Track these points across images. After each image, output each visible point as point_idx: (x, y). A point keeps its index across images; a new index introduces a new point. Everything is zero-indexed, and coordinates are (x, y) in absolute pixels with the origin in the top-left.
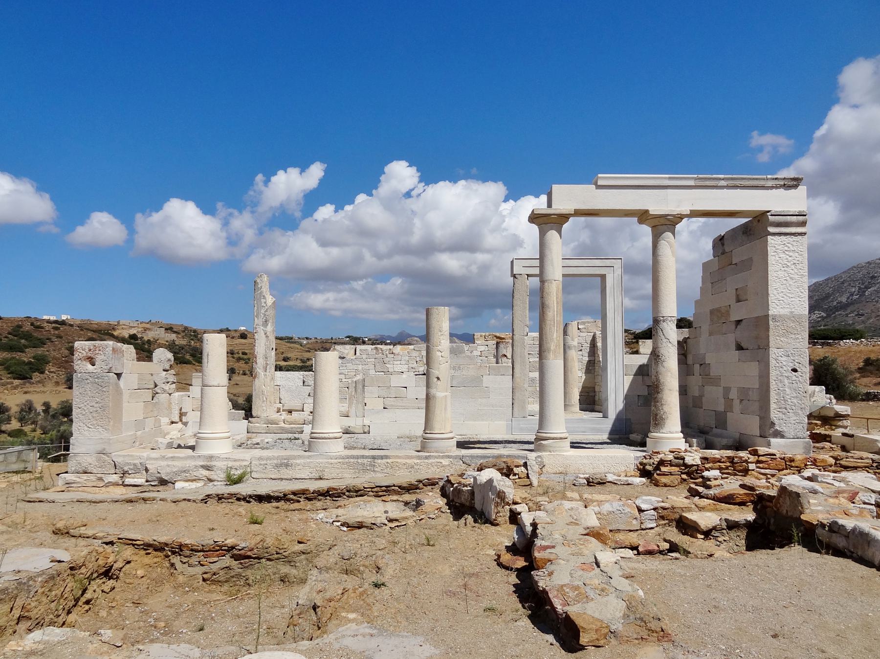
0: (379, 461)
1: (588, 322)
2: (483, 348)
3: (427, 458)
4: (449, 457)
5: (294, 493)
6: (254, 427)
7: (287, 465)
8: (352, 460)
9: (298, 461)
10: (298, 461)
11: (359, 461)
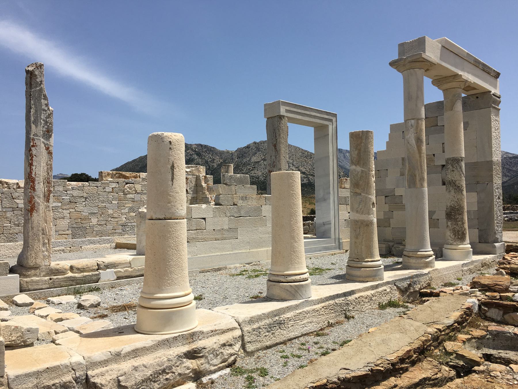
0: (350, 298)
1: (192, 167)
2: (114, 185)
3: (377, 287)
4: (388, 283)
5: (402, 360)
6: (32, 281)
7: (280, 324)
8: (331, 302)
9: (289, 315)
10: (289, 315)
11: (337, 301)
